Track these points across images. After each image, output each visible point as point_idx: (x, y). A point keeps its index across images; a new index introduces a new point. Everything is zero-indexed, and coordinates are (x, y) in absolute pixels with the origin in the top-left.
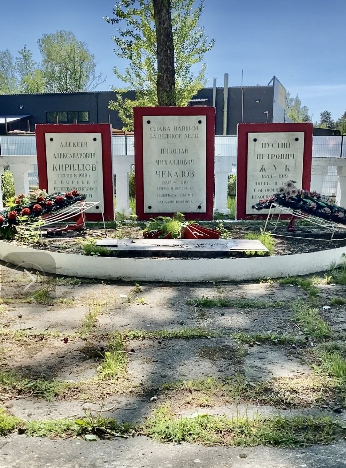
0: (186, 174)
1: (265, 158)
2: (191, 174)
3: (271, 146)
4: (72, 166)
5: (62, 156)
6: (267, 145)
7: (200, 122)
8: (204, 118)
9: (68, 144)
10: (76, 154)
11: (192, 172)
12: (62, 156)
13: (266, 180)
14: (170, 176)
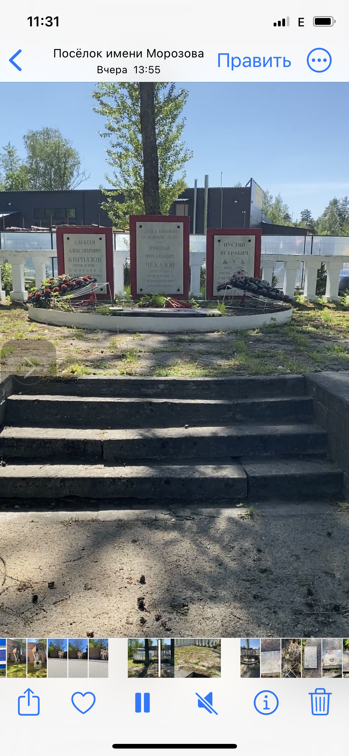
0: (169, 265)
1: (227, 254)
2: (172, 265)
3: (230, 245)
4: (83, 258)
5: (76, 251)
6: (228, 244)
7: (179, 227)
8: (181, 224)
9: (80, 242)
10: (86, 250)
11: (172, 264)
12: (76, 251)
13: (227, 270)
14: (156, 266)
